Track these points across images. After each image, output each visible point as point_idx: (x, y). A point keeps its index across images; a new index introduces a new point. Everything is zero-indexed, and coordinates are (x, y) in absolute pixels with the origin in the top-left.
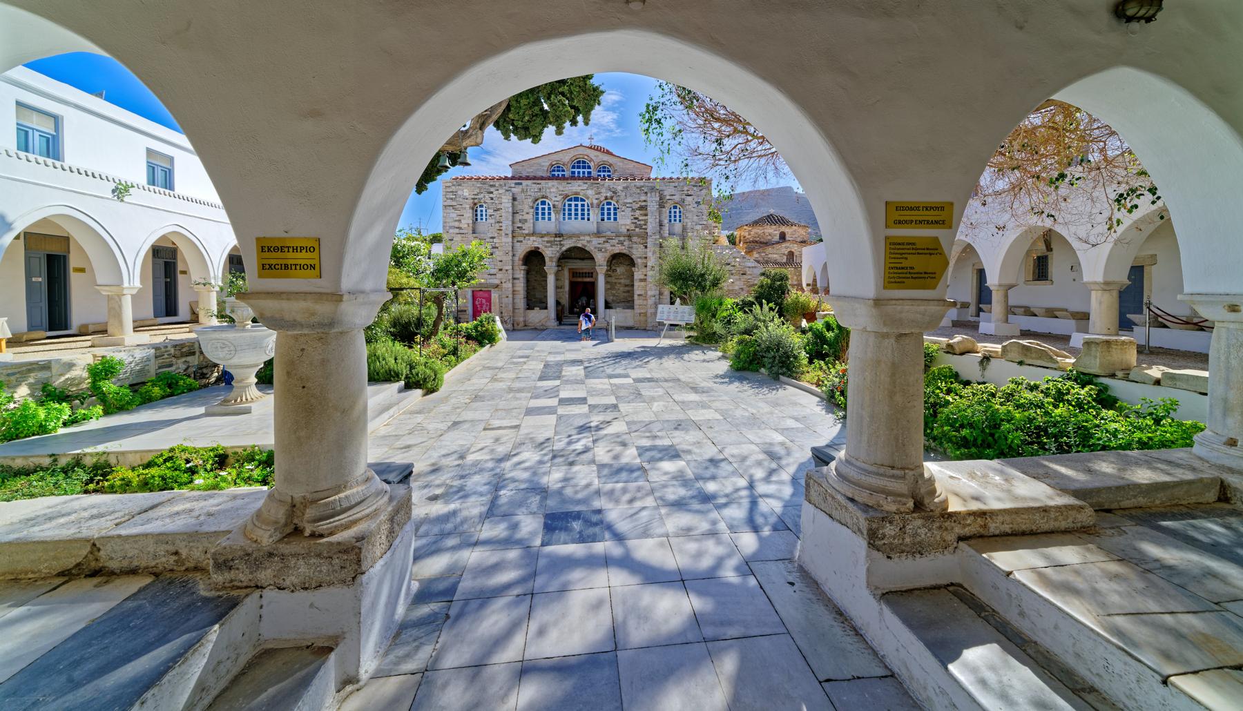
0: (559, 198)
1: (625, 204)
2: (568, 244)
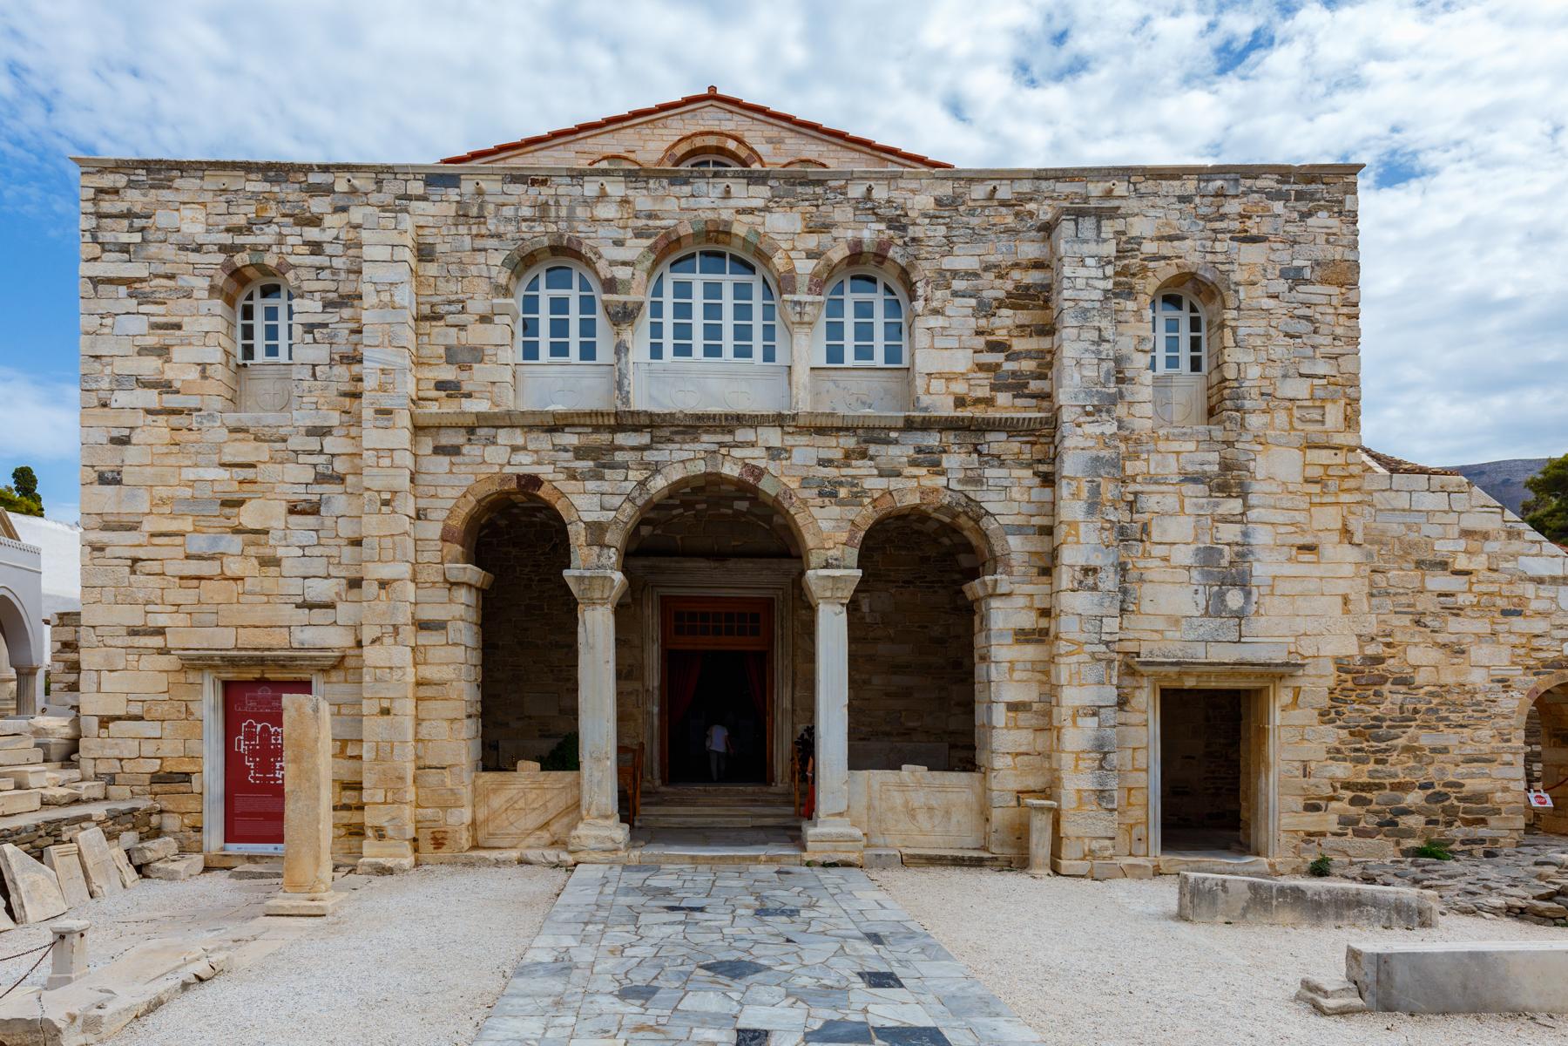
0: (636, 248)
1: (944, 278)
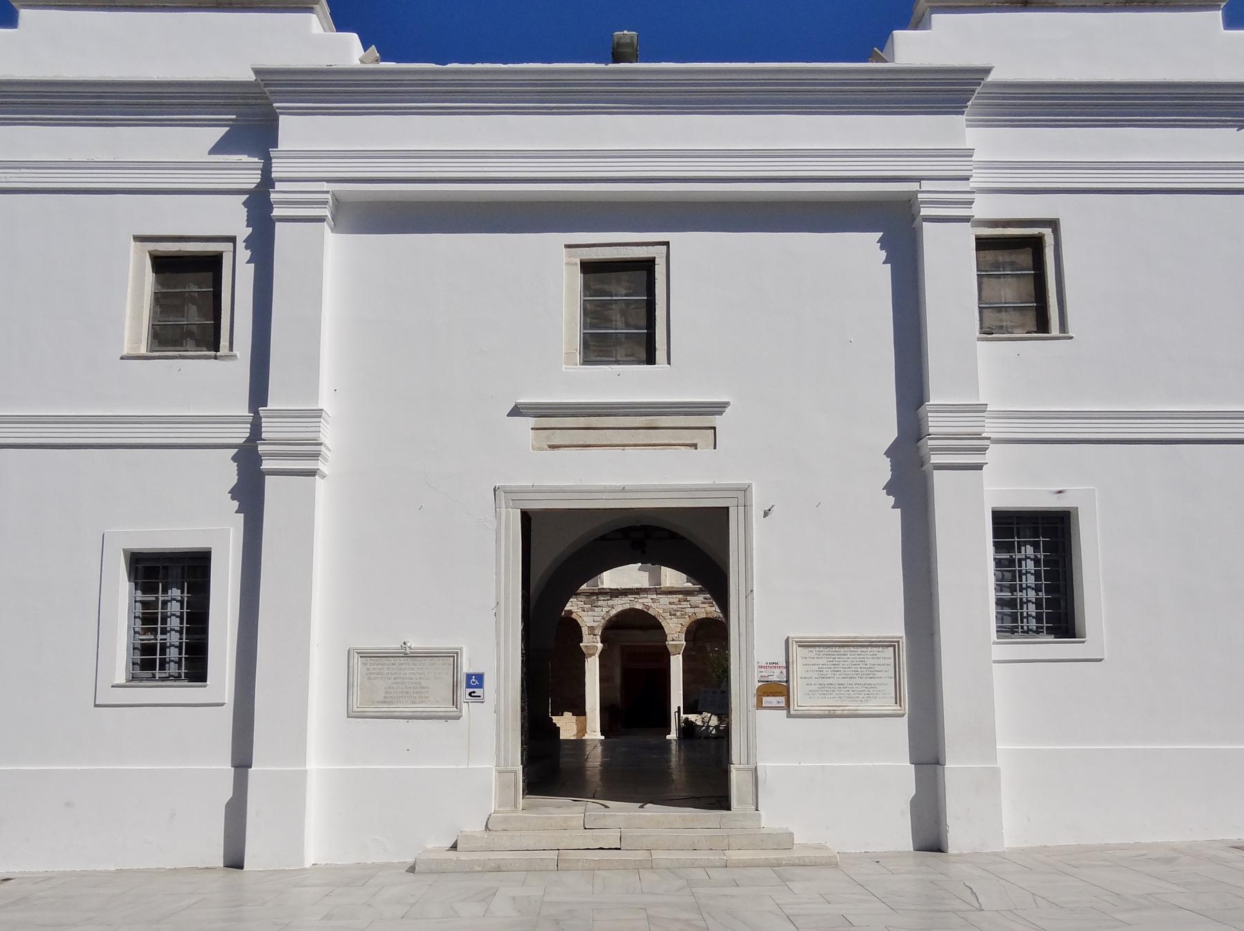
2: (621, 604)
